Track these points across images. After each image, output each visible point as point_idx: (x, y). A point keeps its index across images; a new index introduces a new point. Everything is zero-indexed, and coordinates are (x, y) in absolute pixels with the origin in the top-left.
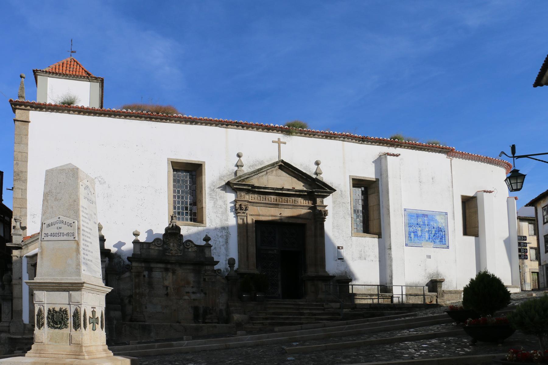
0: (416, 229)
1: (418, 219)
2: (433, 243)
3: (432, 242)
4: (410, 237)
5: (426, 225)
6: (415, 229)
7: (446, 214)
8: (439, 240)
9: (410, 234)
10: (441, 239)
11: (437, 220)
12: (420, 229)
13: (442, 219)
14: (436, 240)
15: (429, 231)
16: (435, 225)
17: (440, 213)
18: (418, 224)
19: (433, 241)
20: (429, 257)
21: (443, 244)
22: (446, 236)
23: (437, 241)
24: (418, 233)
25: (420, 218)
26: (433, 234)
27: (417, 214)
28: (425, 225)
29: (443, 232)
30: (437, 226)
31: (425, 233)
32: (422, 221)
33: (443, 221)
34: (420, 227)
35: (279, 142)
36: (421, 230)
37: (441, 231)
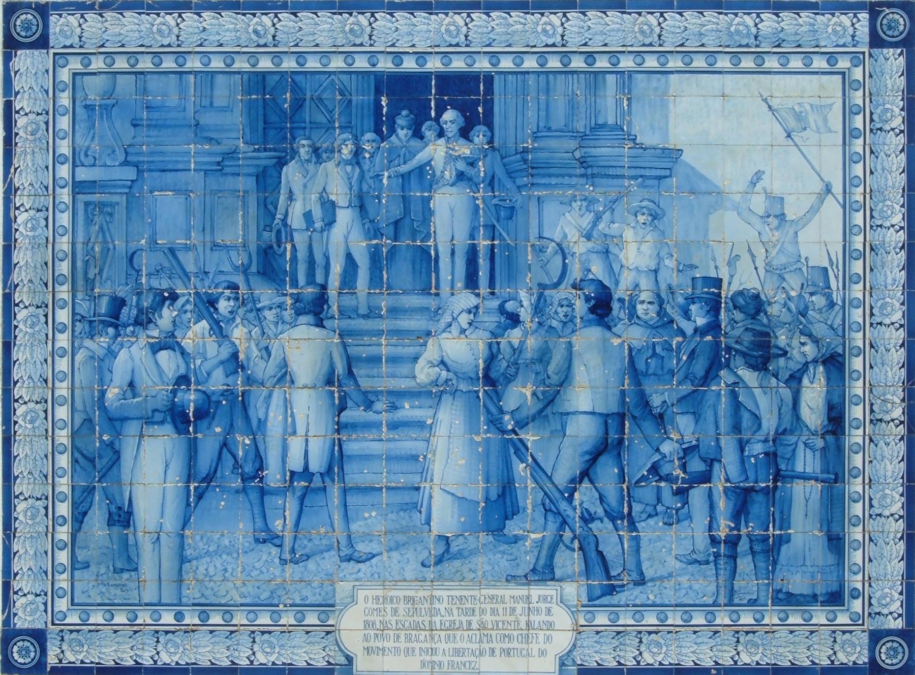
0: (234, 364)
1: (292, 174)
2: (572, 590)
4: (96, 519)
6: (214, 351)
10: (740, 513)
11: (673, 155)
14: (649, 530)
22: (855, 437)
29: (795, 379)
30: (668, 277)
32: (361, 205)
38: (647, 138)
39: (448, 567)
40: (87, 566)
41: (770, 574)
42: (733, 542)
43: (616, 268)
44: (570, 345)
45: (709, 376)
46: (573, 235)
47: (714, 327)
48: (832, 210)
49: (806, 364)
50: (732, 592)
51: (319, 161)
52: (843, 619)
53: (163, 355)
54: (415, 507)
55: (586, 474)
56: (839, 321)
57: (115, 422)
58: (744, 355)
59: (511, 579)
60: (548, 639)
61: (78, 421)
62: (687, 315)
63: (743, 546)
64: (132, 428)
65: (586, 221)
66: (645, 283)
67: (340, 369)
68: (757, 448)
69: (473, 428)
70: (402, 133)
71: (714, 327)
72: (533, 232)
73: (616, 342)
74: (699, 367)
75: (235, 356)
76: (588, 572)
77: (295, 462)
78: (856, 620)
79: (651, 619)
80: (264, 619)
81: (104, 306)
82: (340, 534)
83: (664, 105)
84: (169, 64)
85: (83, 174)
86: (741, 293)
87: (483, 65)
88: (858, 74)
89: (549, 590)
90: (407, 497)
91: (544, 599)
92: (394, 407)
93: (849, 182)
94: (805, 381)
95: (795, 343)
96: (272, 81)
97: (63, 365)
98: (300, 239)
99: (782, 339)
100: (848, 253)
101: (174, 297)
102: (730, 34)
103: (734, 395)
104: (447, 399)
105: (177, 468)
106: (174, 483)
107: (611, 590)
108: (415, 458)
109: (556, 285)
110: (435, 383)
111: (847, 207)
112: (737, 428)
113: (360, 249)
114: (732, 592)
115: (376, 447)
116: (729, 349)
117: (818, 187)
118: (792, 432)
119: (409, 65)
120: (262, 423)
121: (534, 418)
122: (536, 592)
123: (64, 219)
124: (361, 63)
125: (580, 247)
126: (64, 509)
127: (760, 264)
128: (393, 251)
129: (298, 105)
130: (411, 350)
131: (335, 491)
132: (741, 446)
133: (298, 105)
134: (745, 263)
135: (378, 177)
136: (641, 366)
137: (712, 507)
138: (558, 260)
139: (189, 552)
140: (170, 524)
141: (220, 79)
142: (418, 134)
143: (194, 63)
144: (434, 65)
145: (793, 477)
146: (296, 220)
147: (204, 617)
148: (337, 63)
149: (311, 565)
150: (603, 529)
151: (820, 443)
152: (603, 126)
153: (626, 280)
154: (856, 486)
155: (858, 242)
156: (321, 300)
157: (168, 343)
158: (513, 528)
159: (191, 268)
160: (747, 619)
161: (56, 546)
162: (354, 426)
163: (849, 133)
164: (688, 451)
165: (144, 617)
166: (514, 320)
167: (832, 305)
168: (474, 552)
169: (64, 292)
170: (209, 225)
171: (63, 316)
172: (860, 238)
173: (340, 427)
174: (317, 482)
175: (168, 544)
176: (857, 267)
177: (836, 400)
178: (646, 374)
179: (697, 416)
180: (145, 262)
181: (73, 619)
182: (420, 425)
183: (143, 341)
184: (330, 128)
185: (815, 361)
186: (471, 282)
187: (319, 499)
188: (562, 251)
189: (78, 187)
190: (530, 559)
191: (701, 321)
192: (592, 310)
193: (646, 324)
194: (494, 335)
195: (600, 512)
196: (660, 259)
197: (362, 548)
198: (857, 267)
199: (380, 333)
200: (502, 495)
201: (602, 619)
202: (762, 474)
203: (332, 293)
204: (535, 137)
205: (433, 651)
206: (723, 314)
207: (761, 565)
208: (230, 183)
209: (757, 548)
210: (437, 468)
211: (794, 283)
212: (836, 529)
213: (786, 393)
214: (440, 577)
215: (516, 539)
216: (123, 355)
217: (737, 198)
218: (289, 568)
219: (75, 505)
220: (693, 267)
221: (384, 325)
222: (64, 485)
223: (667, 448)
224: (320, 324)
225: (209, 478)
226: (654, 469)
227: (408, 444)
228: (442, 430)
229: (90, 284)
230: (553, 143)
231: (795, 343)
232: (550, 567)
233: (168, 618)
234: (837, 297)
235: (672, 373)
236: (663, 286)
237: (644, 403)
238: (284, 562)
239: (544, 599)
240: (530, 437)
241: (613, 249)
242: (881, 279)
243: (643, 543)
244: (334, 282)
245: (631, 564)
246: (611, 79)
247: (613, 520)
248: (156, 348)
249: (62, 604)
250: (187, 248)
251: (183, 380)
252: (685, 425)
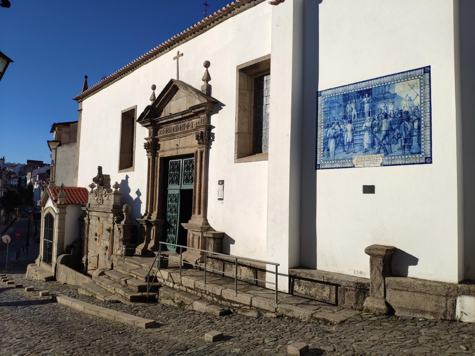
0: (341, 130)
1: (348, 106)
2: (383, 155)
3: (379, 152)
4: (326, 150)
6: (339, 129)
8: (399, 145)
9: (328, 142)
10: (405, 142)
11: (395, 94)
12: (349, 127)
13: (412, 87)
14: (393, 146)
15: (372, 127)
16: (391, 108)
19: (382, 151)
20: (369, 189)
21: (412, 154)
23: (395, 147)
24: (346, 136)
25: (351, 103)
26: (384, 133)
27: (344, 95)
28: (364, 114)
29: (413, 122)
30: (395, 111)
31: (362, 133)
32: (356, 108)
34: (350, 122)
36: (354, 131)
37: (408, 119)
38: (392, 93)
39: (366, 153)
40: (324, 156)
41: (410, 150)
42: (404, 146)
43: (388, 111)
44: (382, 122)
45: (401, 123)
46: (382, 107)
47: (401, 117)
48: (418, 97)
49: (415, 120)
50: (404, 153)
51: (351, 103)
52: (421, 156)
53: (333, 130)
54: (362, 145)
55: (384, 139)
56: (420, 113)
57: (328, 139)
58: (406, 120)
59: (374, 154)
60: (379, 161)
61: (324, 139)
62: (398, 115)
63: (406, 146)
64: (329, 139)
65: (384, 105)
66: (392, 112)
67: (353, 129)
68: (408, 133)
69: (369, 134)
70: (361, 98)
71: (401, 117)
72: (377, 108)
73: (388, 120)
74: (399, 122)
75: (341, 129)
76: (384, 152)
77: (348, 141)
78: (423, 156)
79: (393, 158)
80: (344, 161)
81: (327, 125)
82: (353, 150)
83: (394, 88)
84: (334, 95)
85: (325, 110)
86: (405, 111)
87: (371, 87)
88: (422, 78)
89: (379, 155)
90: (361, 144)
91: (379, 156)
92: (360, 133)
93: (421, 93)
94: (415, 122)
95: (413, 117)
96: (345, 95)
97: (322, 133)
98: (349, 114)
99: (411, 117)
100: (421, 103)
101: (334, 123)
102: (403, 76)
103: (404, 126)
104: (366, 131)
105: (334, 143)
106: (334, 145)
107: (388, 154)
108: (362, 139)
109: (380, 114)
110: (365, 129)
111: (421, 97)
112: (405, 130)
113: (356, 113)
114: (404, 153)
115: (357, 138)
116: (404, 119)
117: (416, 95)
118: (413, 130)
119: (362, 89)
120: (344, 137)
121: (377, 132)
122: (378, 155)
123: (323, 116)
124: (356, 90)
125: (383, 109)
126: (322, 150)
127: (408, 107)
128: (360, 113)
129: (349, 97)
130: (362, 125)
131: (352, 144)
132: (405, 132)
133: (349, 97)
134: (406, 107)
135: (358, 104)
136: (391, 123)
137: (401, 141)
138: (380, 111)
139: (336, 154)
140: (333, 150)
141: (340, 96)
142: (363, 98)
143: (337, 94)
144: (365, 89)
145: (413, 136)
146: (348, 111)
147: (337, 161)
148: (353, 91)
149: (350, 154)
150: (386, 146)
151: (417, 131)
152: (386, 92)
153: (389, 112)
154: (423, 136)
155: (422, 101)
156: (351, 120)
157: (334, 129)
158: (375, 147)
159: (336, 119)
160: (407, 157)
161: (321, 154)
162: (355, 136)
163: (421, 86)
164: (398, 134)
165: (331, 162)
166: (375, 119)
167: (419, 111)
168: (370, 150)
169: (322, 124)
170: (338, 113)
171: (322, 127)
172: (423, 101)
173: (353, 136)
174: (350, 144)
175: (333, 153)
176: (422, 105)
177: (419, 124)
178: (392, 124)
179: (399, 129)
180: (331, 119)
181: (323, 163)
182: (363, 135)
183: (331, 128)
184: (352, 99)
185: (416, 119)
186: (369, 116)
187: (351, 145)
188: (381, 110)
189: (324, 112)
190: (377, 151)
191: (400, 116)
192: (385, 117)
193: (392, 118)
194: (372, 122)
195: (386, 144)
196: (394, 108)
197: (356, 151)
198: (422, 105)
199: (358, 124)
200: (373, 143)
201: (386, 158)
202: (408, 136)
203: (352, 119)
204: (377, 95)
205: (365, 164)
206: (403, 115)
207: (409, 149)
208: (341, 108)
209: (408, 147)
210: (365, 140)
211: (413, 109)
212: (419, 143)
213: (412, 124)
214: (365, 154)
215: (375, 148)
216: (329, 131)
217: (404, 98)
218: (347, 154)
219: (323, 149)
220: (398, 109)
221: (359, 123)
222: (322, 147)
223: (395, 134)
224: (351, 124)
225: (338, 144)
226: (393, 137)
227: (361, 137)
228: (365, 135)
229: (325, 123)
230: (380, 96)
231: (413, 117)
232: (379, 151)
233: (333, 162)
234: (419, 110)
235: (396, 124)
236: (394, 112)
237: (392, 128)
238: (346, 154)
239: (379, 156)
240: (377, 135)
241: (388, 108)
242: (426, 106)
243: (392, 147)
244: (353, 118)
245: (390, 150)
246: (387, 86)
247: (388, 145)
248: (332, 129)
249: (322, 161)
250: (336, 117)
251: (335, 133)
252: (397, 130)
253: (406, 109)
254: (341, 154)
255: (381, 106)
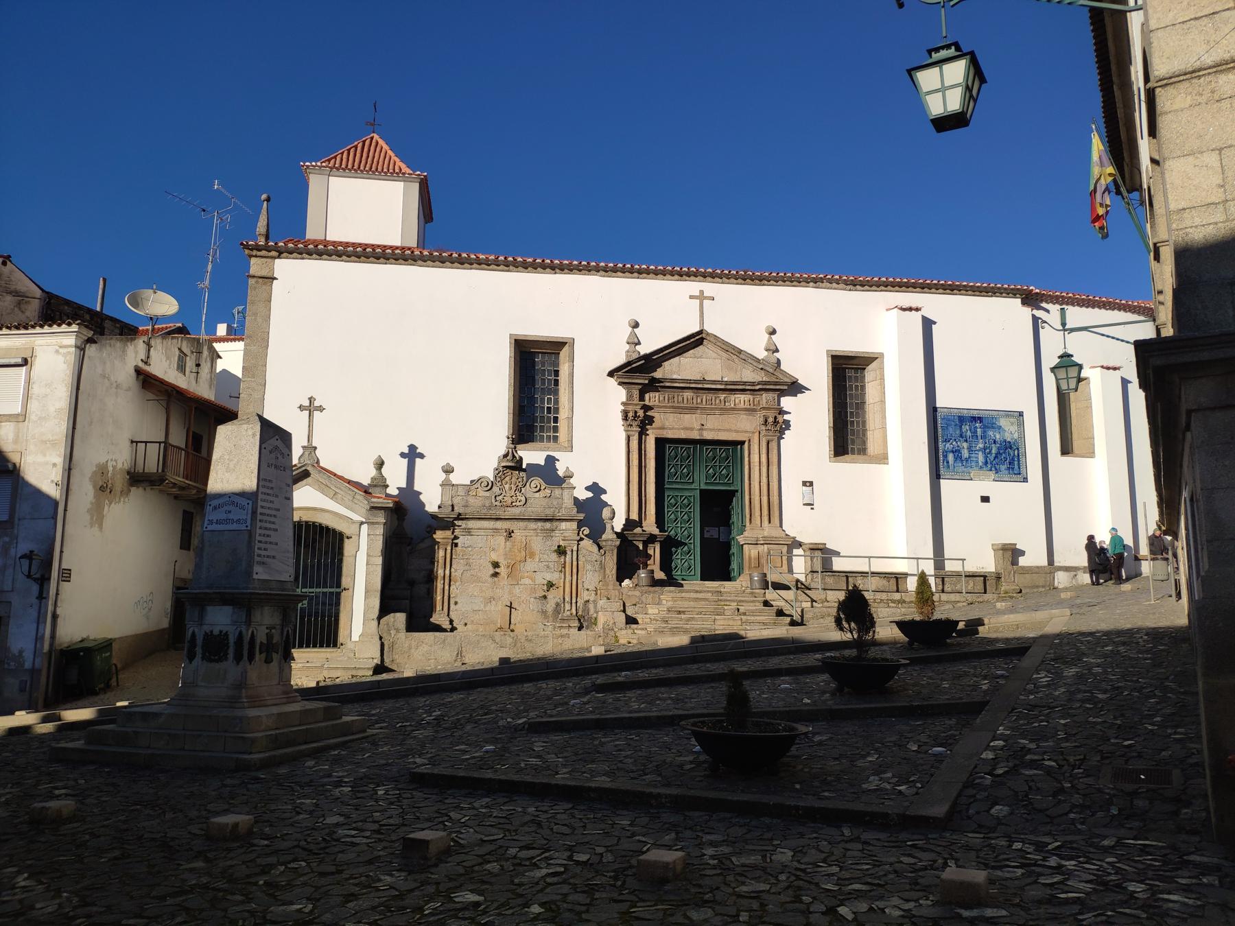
3: (991, 470)
5: (979, 437)
7: (1021, 414)
12: (965, 445)
13: (1012, 424)
15: (985, 449)
16: (998, 436)
17: (1008, 414)
18: (961, 436)
19: (993, 469)
20: (985, 499)
23: (1003, 467)
26: (994, 455)
28: (977, 436)
33: (1014, 429)
34: (966, 441)
35: (701, 297)
36: (970, 449)
37: (1011, 448)
253: (1009, 440)
254: (961, 469)
255: (991, 433)
